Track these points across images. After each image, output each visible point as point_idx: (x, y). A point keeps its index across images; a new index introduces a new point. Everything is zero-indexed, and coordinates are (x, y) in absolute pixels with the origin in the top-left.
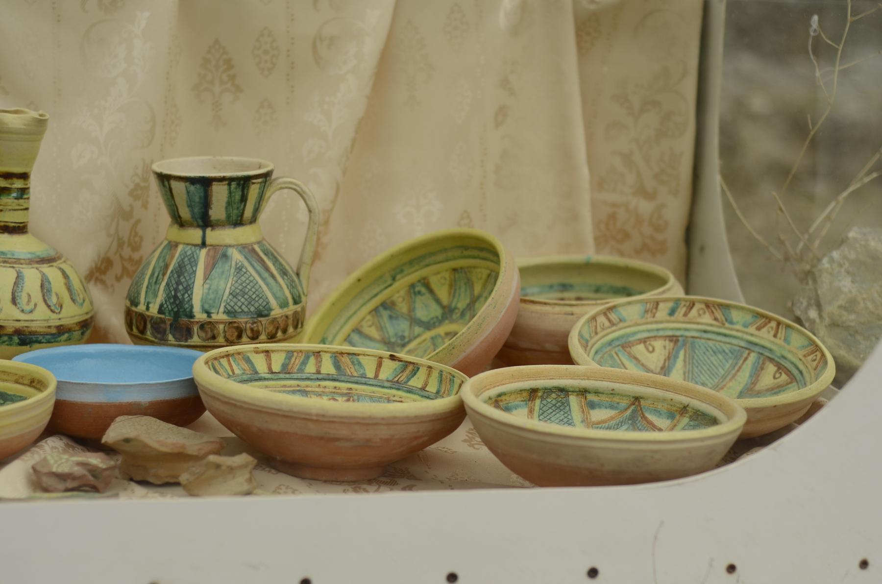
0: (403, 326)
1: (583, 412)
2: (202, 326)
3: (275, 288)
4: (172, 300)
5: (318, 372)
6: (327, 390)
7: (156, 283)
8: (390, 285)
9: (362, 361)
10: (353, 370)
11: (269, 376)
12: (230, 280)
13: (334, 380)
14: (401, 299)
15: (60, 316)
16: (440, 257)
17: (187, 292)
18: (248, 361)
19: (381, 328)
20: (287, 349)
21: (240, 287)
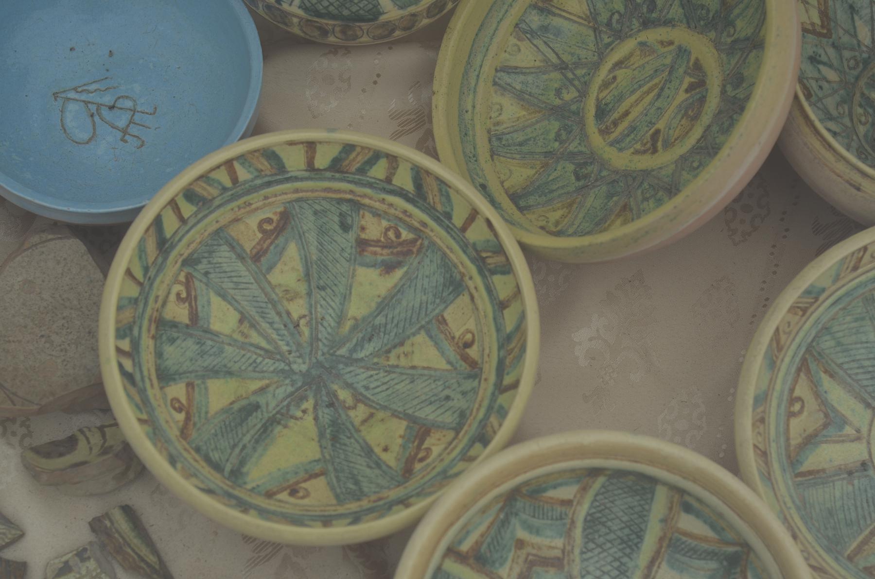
1: (671, 509)
5: (389, 180)
6: (392, 211)
10: (437, 199)
13: (408, 199)
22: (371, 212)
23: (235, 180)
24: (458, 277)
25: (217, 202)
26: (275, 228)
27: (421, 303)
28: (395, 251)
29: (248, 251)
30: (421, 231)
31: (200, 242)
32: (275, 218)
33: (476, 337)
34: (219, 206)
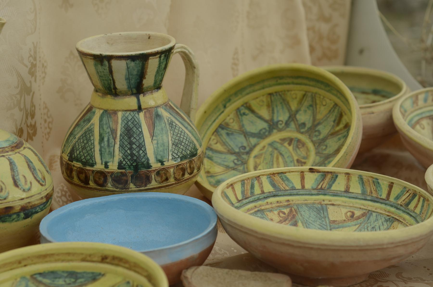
0: (241, 140)
2: (158, 173)
4: (129, 157)
5: (263, 192)
6: (274, 205)
7: (108, 145)
8: (223, 112)
9: (288, 177)
10: (284, 185)
12: (169, 134)
13: (275, 196)
14: (232, 121)
16: (257, 87)
17: (141, 149)
19: (224, 144)
20: (240, 179)
21: (177, 138)
22: (268, 211)
24: (319, 206)
27: (320, 225)
28: (289, 219)
30: (289, 204)
33: (352, 210)
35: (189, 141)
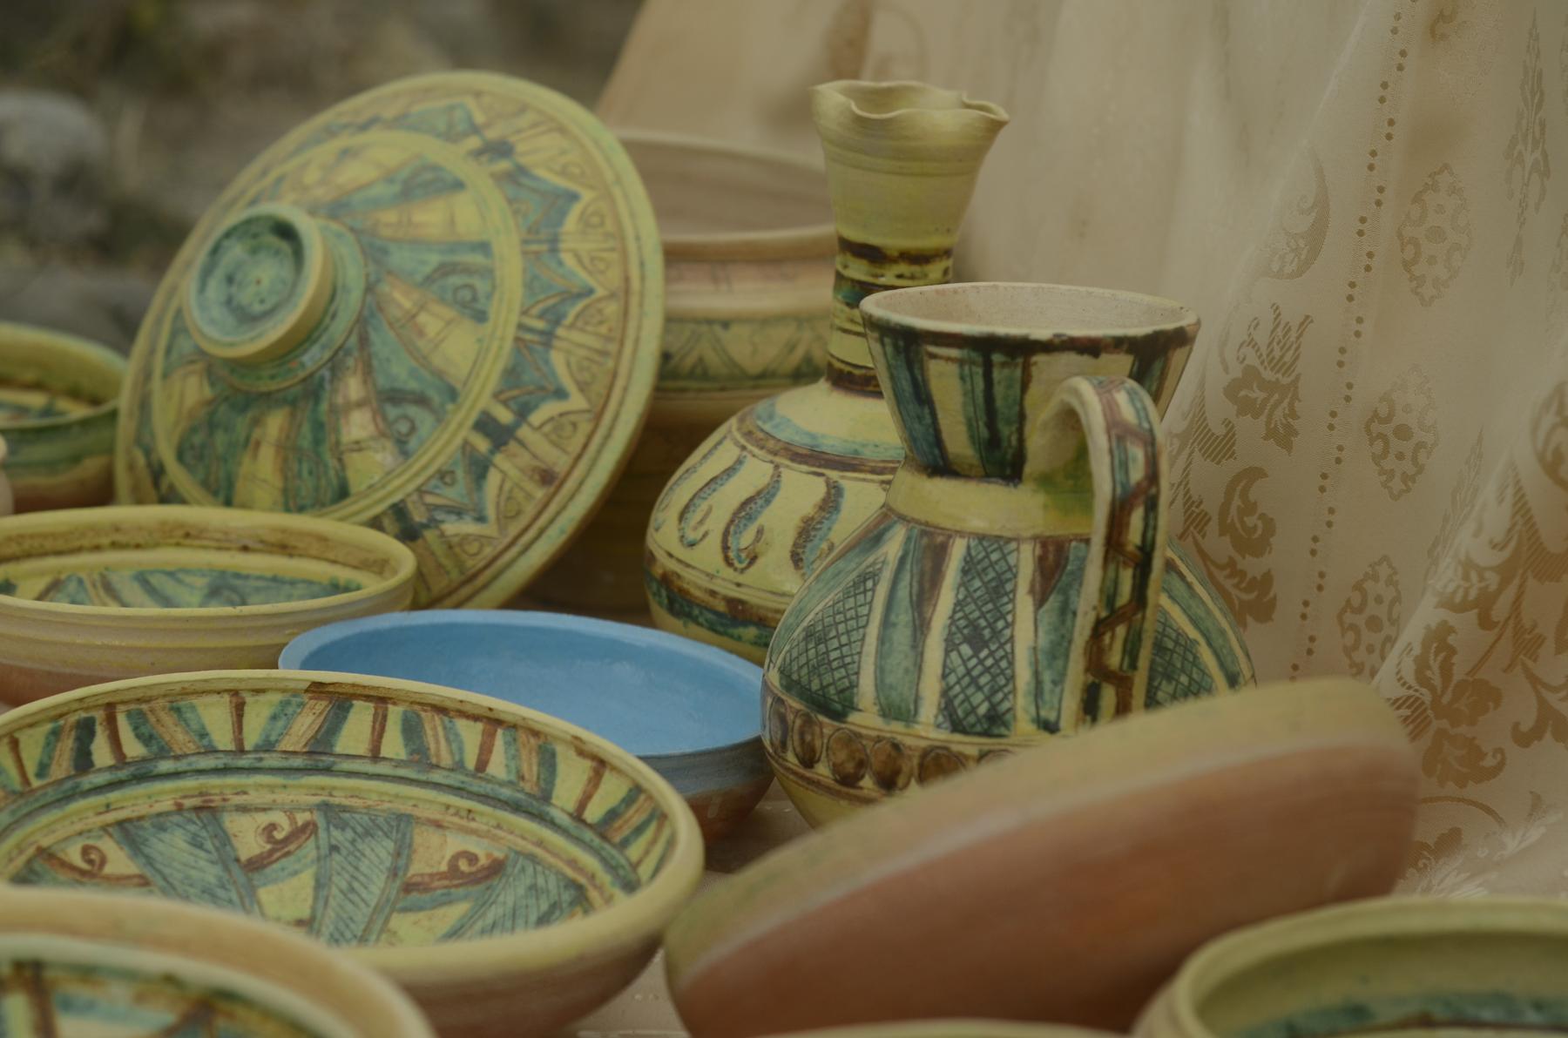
3: (900, 658)
11: (564, 820)
15: (741, 579)
18: (548, 760)
23: (482, 765)
25: (436, 776)
26: (471, 874)
29: (411, 872)
31: (368, 807)
32: (483, 861)
34: (437, 786)
35: (842, 657)
